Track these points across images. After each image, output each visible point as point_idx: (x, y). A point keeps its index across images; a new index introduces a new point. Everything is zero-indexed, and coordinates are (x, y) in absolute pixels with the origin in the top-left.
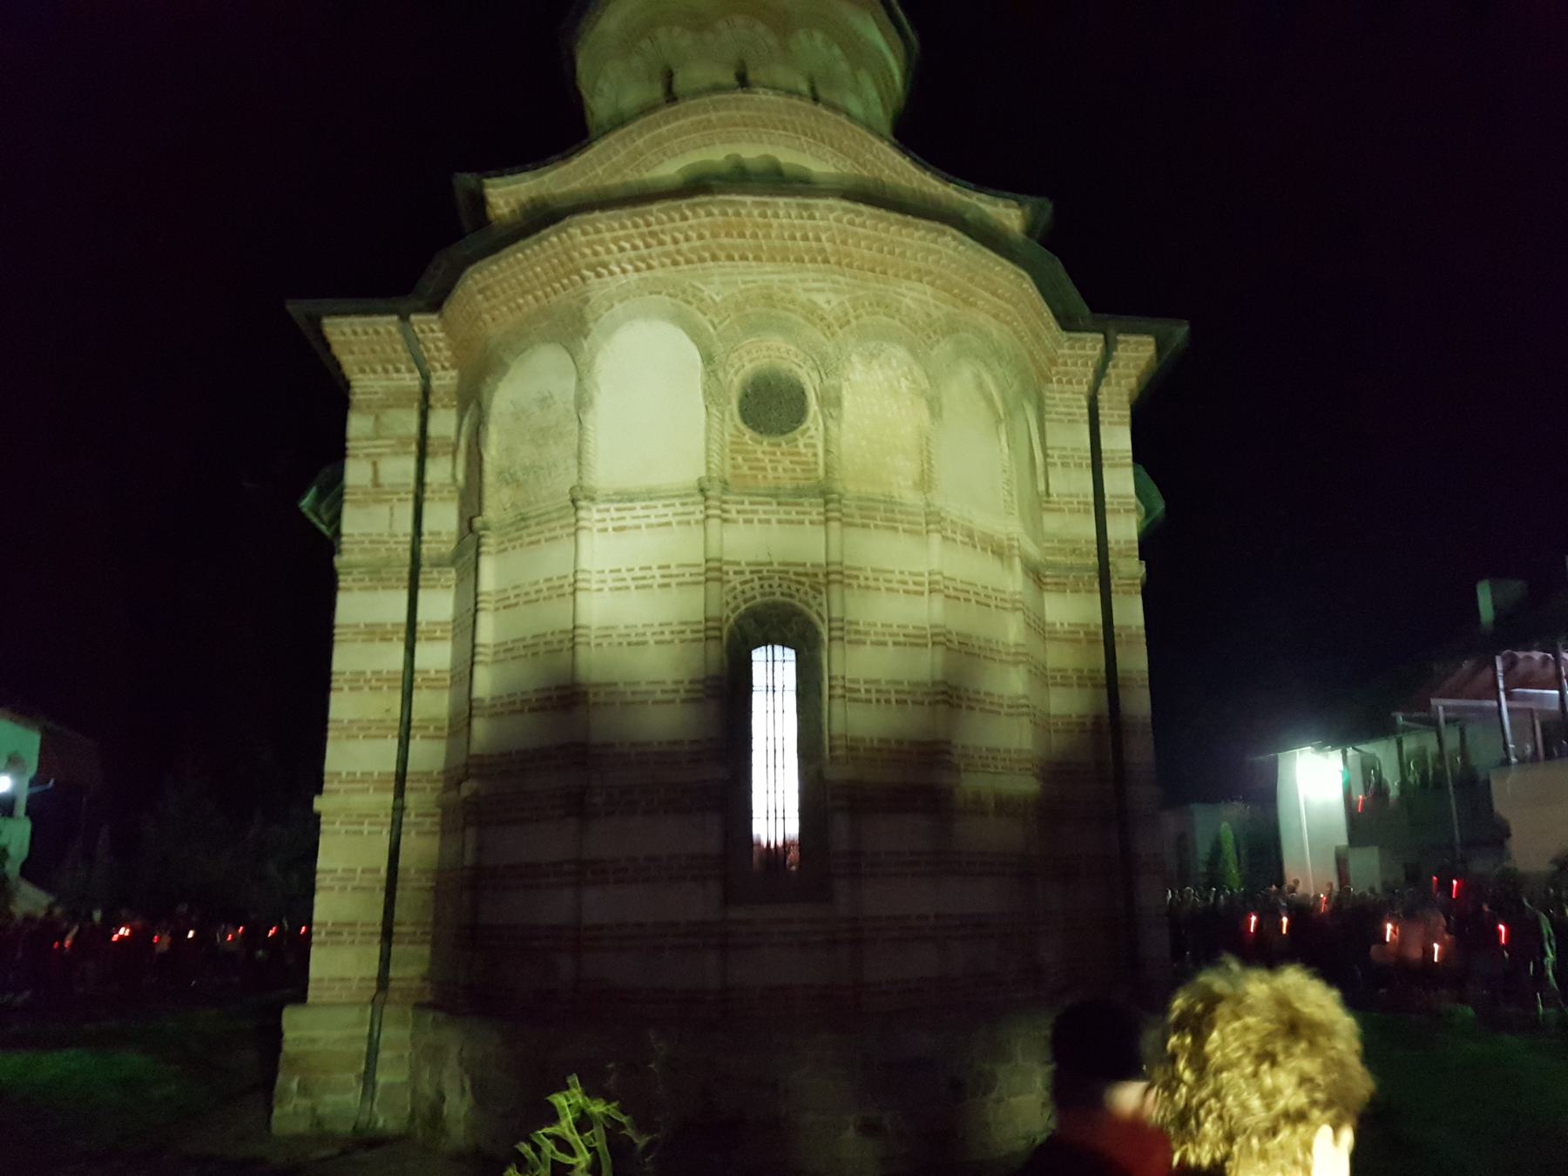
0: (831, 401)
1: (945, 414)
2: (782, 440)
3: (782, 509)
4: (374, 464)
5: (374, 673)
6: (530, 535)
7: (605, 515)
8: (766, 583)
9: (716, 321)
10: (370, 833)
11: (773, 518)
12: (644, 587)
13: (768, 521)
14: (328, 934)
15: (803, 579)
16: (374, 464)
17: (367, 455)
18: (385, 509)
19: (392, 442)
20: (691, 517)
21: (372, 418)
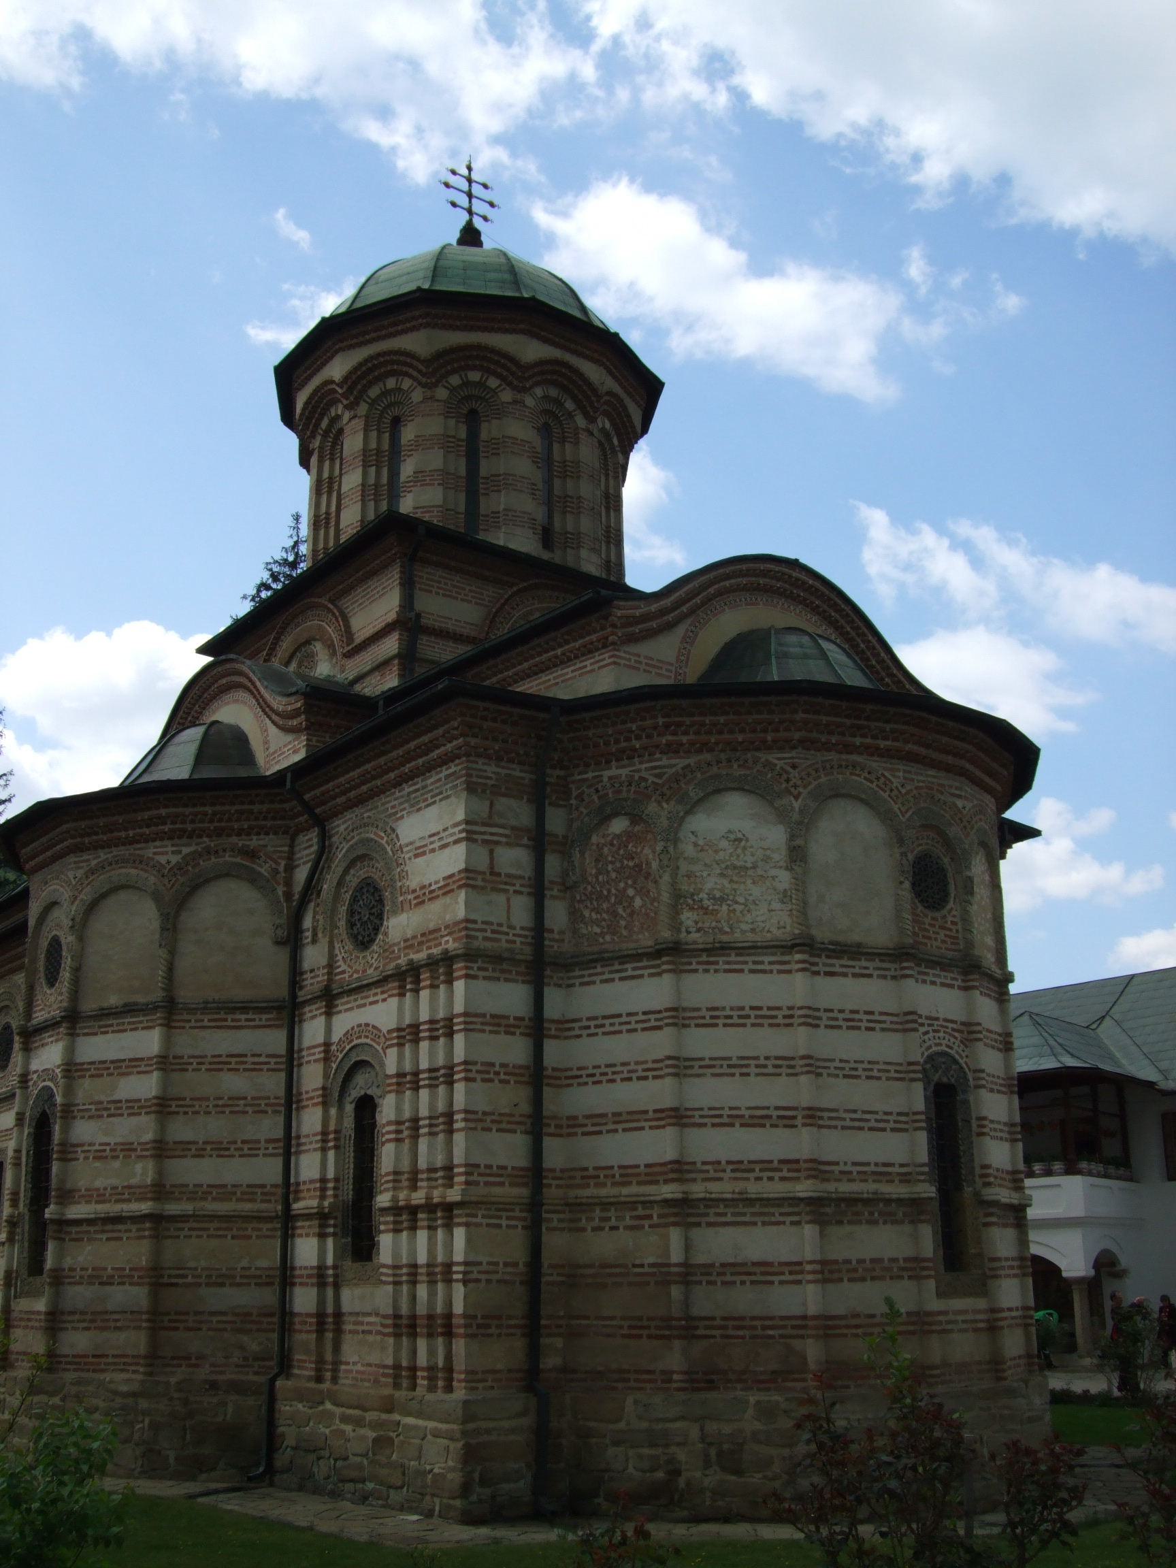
2: (937, 914)
3: (943, 974)
4: (491, 852)
5: (503, 1065)
6: (728, 963)
7: (816, 960)
8: (937, 1035)
9: (903, 809)
10: (508, 1226)
11: (938, 980)
12: (853, 1028)
13: (933, 983)
14: (479, 1326)
15: (956, 1034)
16: (491, 852)
17: (485, 842)
18: (501, 899)
19: (507, 832)
20: (887, 973)
21: (487, 803)
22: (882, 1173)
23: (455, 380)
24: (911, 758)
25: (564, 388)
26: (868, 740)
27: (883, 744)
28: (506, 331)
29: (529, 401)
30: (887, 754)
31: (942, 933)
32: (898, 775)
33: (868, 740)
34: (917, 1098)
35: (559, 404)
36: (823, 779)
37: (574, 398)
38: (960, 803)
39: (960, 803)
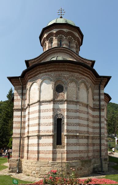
0: (66, 88)
1: (80, 90)
22: (47, 131)
23: (49, 39)
24: (54, 71)
25: (62, 34)
26: (48, 70)
27: (50, 70)
28: (52, 30)
29: (57, 38)
30: (51, 71)
31: (61, 96)
32: (53, 74)
33: (48, 70)
34: (51, 121)
35: (62, 36)
36: (42, 77)
37: (64, 35)
38: (65, 76)
39: (65, 76)
